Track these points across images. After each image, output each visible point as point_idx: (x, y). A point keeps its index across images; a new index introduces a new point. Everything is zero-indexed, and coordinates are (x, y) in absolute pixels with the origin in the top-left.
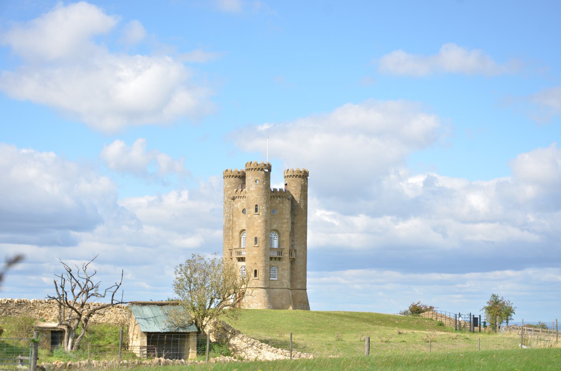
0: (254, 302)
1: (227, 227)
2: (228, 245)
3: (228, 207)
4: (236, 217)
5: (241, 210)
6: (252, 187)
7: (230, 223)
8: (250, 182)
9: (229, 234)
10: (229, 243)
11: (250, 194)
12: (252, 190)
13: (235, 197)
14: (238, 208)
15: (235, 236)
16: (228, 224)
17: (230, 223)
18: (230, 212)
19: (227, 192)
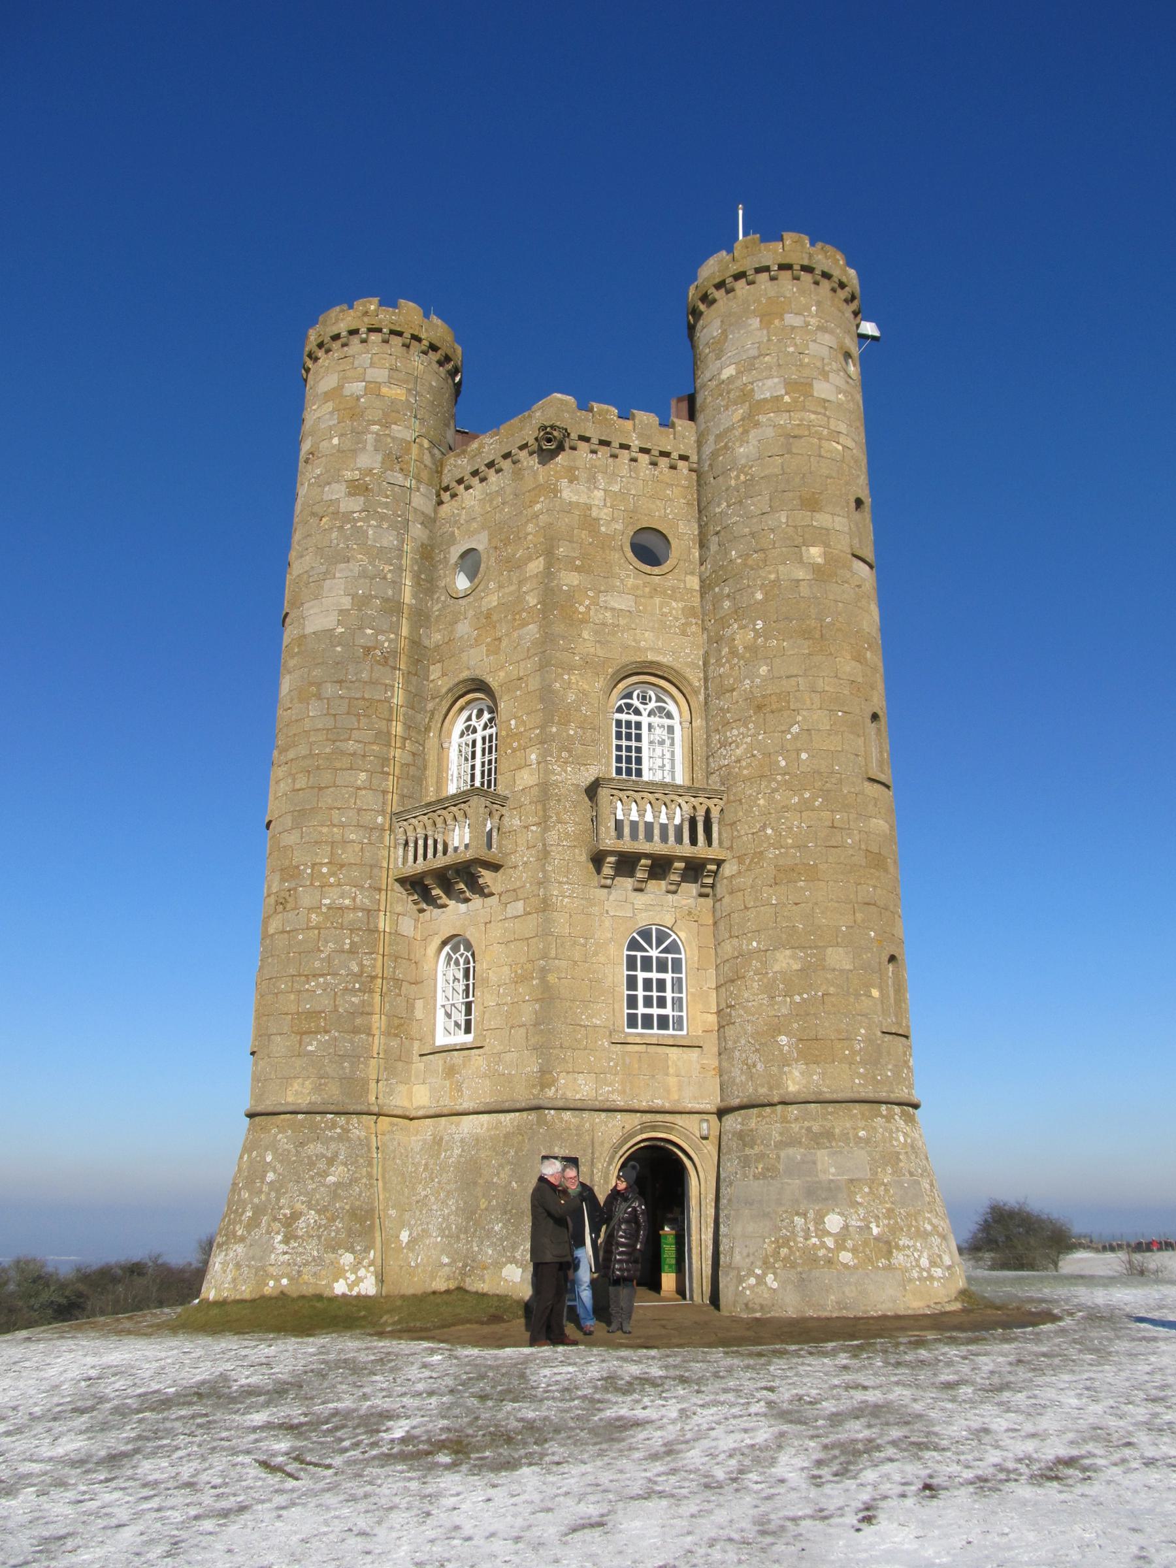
0: (929, 1227)
1: (368, 650)
2: (371, 773)
3: (383, 517)
4: (578, 569)
5: (619, 530)
6: (827, 379)
7: (398, 625)
8: (812, 345)
9: (388, 700)
10: (385, 761)
11: (813, 416)
12: (832, 398)
13: (574, 436)
14: (594, 514)
15: (571, 697)
16: (379, 631)
17: (395, 628)
18: (400, 557)
19: (387, 426)
